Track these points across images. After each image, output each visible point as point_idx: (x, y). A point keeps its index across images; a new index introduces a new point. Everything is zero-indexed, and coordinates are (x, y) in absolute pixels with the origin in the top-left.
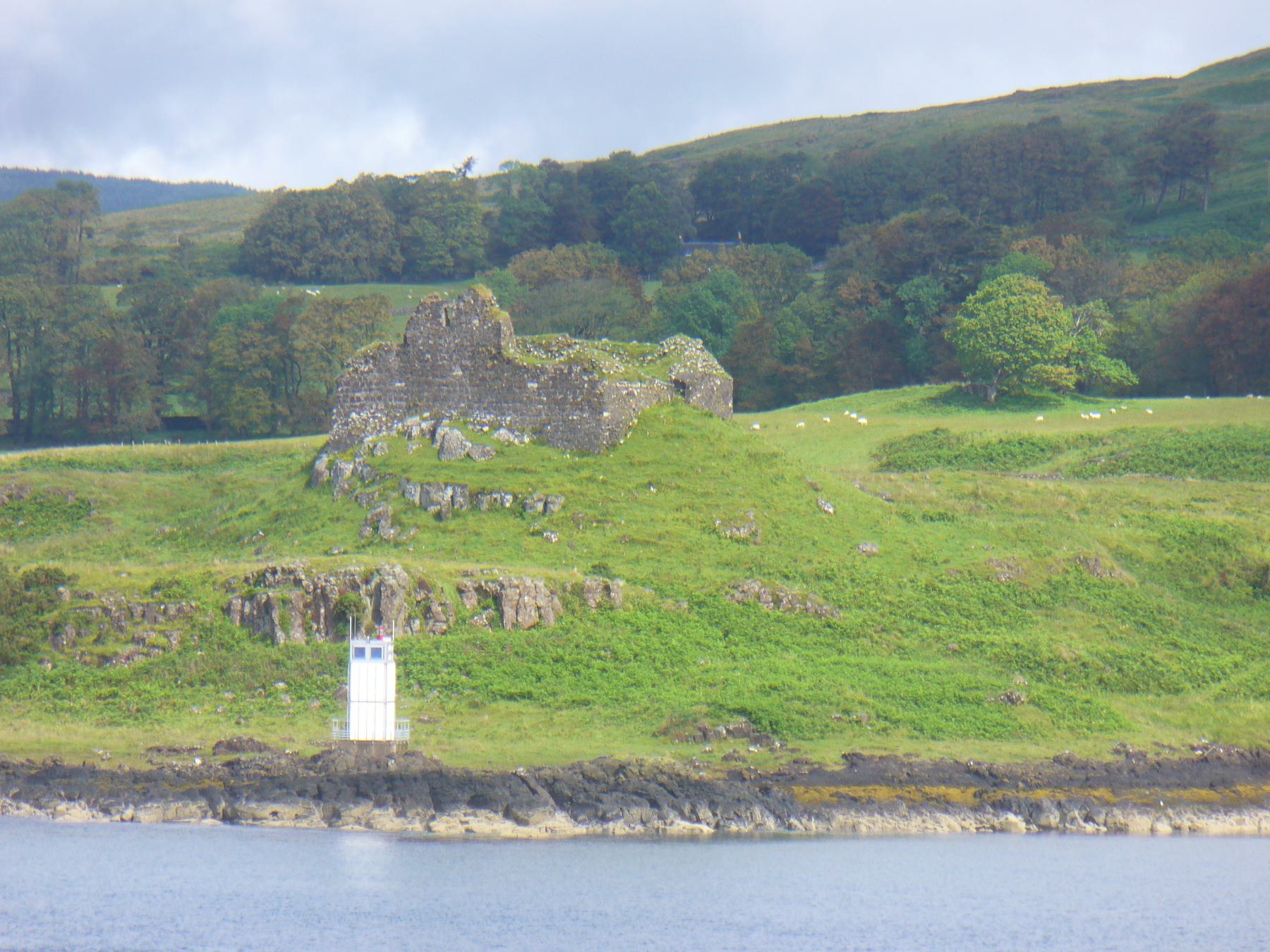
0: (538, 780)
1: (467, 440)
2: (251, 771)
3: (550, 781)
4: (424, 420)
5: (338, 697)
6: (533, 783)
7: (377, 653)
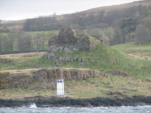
0: (88, 100)
1: (69, 50)
2: (42, 100)
3: (90, 101)
4: (62, 47)
5: (54, 89)
6: (87, 101)
7: (61, 82)
